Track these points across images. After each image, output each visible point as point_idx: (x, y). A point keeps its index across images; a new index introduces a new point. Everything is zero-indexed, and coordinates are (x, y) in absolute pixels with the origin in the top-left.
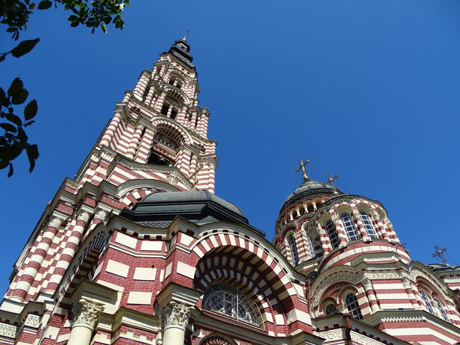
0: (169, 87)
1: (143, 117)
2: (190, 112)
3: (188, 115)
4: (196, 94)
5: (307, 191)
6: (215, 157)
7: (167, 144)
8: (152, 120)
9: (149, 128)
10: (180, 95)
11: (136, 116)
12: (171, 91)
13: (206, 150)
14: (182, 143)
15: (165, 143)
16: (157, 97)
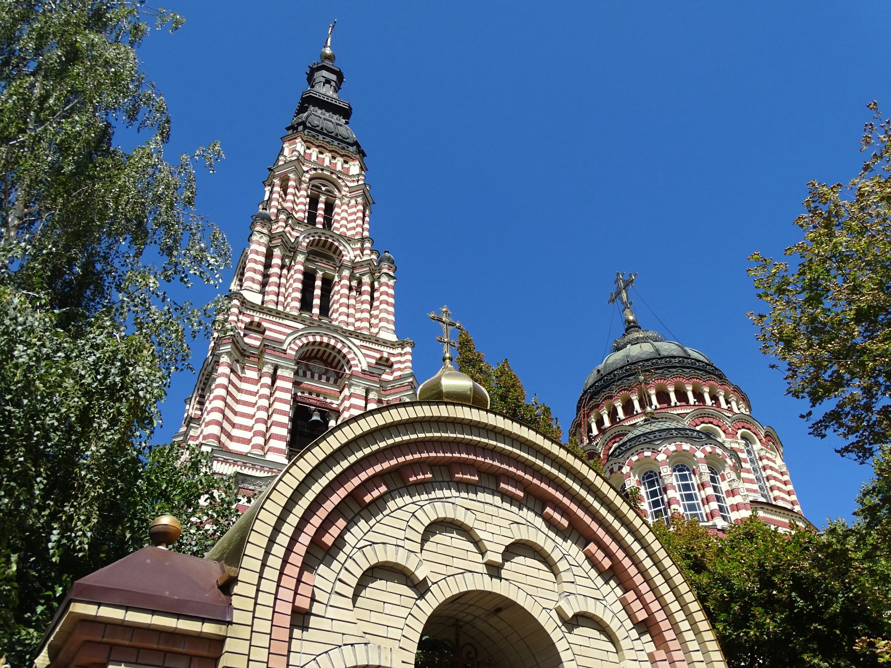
0: (310, 234)
1: (268, 346)
2: (358, 275)
3: (354, 283)
4: (367, 212)
5: (621, 368)
6: (412, 382)
7: (320, 378)
8: (284, 347)
9: (282, 367)
10: (332, 244)
11: (256, 339)
12: (314, 240)
13: (395, 366)
14: (347, 371)
15: (316, 376)
16: (288, 264)
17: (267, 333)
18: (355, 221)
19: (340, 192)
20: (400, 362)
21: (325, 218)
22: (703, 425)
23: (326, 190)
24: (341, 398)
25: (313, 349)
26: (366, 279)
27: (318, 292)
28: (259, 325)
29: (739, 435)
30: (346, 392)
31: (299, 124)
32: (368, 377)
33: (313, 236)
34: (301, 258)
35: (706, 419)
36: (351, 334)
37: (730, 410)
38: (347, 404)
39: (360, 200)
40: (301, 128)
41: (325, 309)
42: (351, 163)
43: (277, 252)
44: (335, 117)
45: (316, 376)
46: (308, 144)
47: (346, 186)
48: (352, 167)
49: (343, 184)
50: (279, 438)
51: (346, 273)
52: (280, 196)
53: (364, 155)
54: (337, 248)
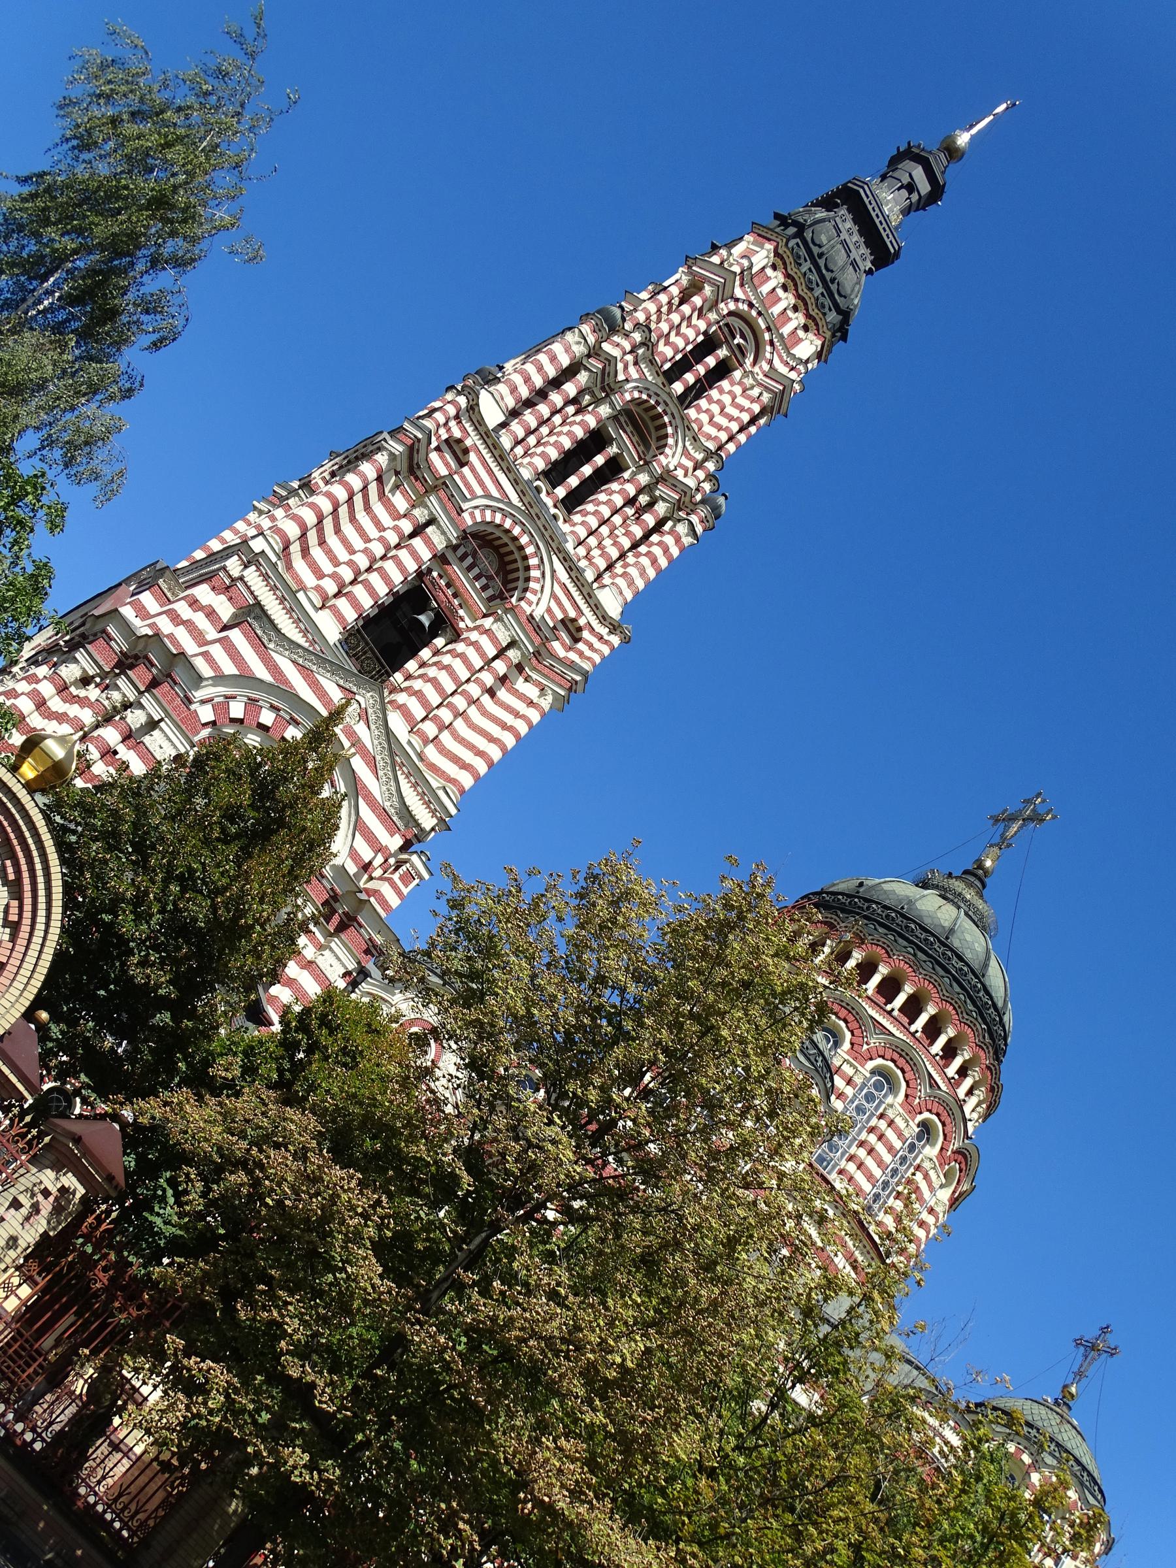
0: (648, 389)
1: (447, 487)
2: (657, 493)
3: (643, 499)
4: (762, 421)
5: (886, 907)
6: (576, 682)
7: (477, 578)
8: (465, 506)
9: (439, 527)
10: (664, 426)
11: (447, 464)
12: (646, 401)
13: (581, 646)
14: (514, 600)
15: (476, 571)
16: (585, 403)
17: (466, 470)
18: (731, 419)
19: (755, 363)
21: (698, 381)
22: (891, 1064)
23: (738, 345)
25: (500, 538)
26: (661, 508)
27: (587, 470)
28: (466, 451)
29: (919, 1118)
30: (488, 622)
31: (795, 223)
32: (529, 628)
33: (650, 396)
34: (604, 410)
35: (901, 1062)
36: (565, 560)
37: (954, 1084)
38: (474, 636)
39: (766, 397)
40: (792, 230)
41: (573, 502)
42: (811, 336)
43: (583, 377)
44: (863, 250)
45: (476, 571)
46: (779, 261)
47: (770, 362)
48: (806, 343)
49: (768, 355)
50: (355, 603)
51: (644, 479)
52: (670, 303)
53: (844, 338)
54: (666, 436)
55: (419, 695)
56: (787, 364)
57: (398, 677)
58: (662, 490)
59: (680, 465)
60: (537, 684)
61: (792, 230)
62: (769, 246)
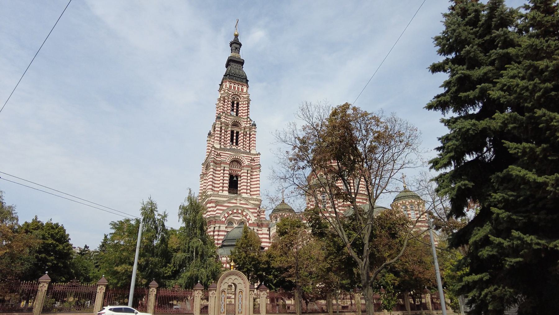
3: (245, 134)
14: (243, 165)
15: (235, 166)
20: (257, 160)
21: (236, 110)
24: (241, 172)
26: (248, 132)
27: (235, 138)
30: (242, 171)
31: (227, 75)
34: (230, 129)
38: (242, 175)
41: (237, 144)
43: (223, 128)
45: (235, 166)
46: (230, 82)
47: (242, 97)
51: (242, 132)
55: (243, 189)
56: (245, 94)
57: (239, 189)
58: (246, 130)
59: (245, 124)
60: (256, 171)
61: (228, 76)
62: (228, 82)
